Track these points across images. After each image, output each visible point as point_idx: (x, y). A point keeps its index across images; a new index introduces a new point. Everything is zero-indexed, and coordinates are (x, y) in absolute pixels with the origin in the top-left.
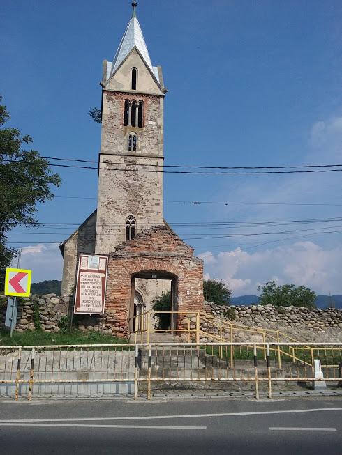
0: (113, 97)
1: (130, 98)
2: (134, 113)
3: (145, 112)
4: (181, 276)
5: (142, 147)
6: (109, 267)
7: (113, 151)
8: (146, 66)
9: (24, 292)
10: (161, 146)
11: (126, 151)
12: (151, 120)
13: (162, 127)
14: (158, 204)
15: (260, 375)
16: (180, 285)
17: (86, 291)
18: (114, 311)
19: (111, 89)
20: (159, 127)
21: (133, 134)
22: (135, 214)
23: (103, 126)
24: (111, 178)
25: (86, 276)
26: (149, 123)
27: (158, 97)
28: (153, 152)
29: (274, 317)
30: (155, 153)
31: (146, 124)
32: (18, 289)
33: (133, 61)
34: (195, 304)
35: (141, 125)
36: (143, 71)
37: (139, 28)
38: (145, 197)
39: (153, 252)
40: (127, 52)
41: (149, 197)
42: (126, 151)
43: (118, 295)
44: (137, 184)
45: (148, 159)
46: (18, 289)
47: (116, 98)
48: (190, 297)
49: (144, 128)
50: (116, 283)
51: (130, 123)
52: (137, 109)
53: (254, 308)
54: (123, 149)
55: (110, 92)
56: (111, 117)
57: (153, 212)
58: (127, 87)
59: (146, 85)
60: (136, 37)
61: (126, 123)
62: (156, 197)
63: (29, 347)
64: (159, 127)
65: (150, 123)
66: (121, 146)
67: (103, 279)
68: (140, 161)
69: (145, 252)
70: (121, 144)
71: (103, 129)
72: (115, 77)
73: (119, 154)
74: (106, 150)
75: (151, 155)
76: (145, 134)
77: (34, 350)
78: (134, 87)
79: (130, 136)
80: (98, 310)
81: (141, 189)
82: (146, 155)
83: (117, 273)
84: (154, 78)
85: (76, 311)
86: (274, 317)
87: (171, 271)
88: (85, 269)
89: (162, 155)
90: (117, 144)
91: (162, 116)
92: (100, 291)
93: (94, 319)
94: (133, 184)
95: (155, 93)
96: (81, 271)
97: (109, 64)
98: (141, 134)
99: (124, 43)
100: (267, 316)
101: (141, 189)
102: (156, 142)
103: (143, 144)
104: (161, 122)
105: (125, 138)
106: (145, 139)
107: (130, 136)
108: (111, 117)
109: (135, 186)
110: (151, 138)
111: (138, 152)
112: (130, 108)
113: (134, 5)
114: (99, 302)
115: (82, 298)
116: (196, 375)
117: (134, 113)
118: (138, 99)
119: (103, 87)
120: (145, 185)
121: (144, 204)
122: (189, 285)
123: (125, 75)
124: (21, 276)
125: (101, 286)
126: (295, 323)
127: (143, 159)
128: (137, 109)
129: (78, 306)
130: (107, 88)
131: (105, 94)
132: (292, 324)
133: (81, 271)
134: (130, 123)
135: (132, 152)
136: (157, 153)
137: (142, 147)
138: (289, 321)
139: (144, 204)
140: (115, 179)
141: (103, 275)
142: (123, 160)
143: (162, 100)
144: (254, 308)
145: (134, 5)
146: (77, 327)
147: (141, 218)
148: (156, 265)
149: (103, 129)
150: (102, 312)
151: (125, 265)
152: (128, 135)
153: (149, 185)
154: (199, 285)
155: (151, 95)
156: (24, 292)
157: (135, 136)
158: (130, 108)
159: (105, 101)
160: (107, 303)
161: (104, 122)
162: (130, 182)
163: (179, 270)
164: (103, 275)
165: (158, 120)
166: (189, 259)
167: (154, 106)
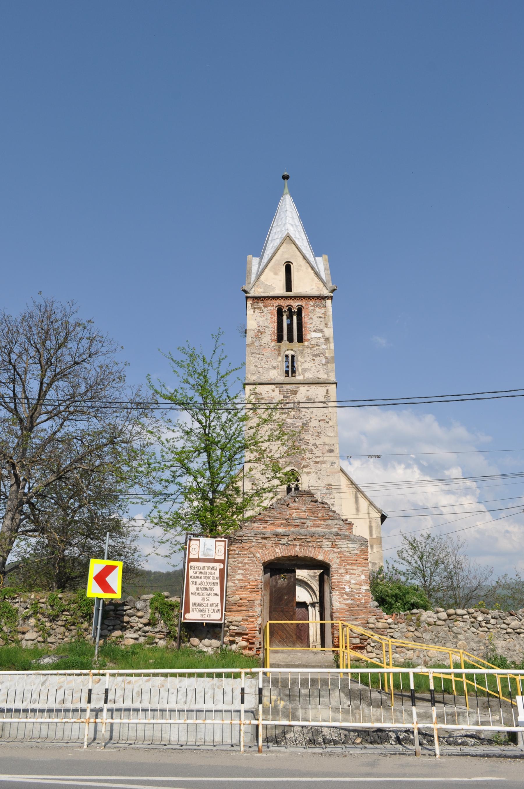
0: (261, 304)
1: (284, 303)
2: (290, 324)
3: (306, 321)
4: (334, 566)
5: (305, 371)
6: (228, 554)
7: (263, 379)
8: (305, 258)
9: (113, 592)
10: (332, 366)
11: (281, 378)
12: (315, 331)
13: (332, 340)
14: (331, 451)
15: (440, 718)
16: (335, 578)
17: (197, 588)
18: (240, 618)
19: (257, 294)
20: (327, 340)
21: (290, 353)
22: (298, 467)
23: (249, 346)
25: (197, 567)
26: (311, 335)
27: (323, 298)
28: (320, 376)
29: (483, 624)
30: (323, 376)
31: (308, 337)
32: (106, 588)
33: (287, 253)
34: (358, 606)
35: (300, 339)
36: (300, 266)
37: (293, 205)
38: (312, 441)
39: (292, 529)
40: (278, 241)
41: (318, 442)
42: (281, 378)
43: (245, 594)
44: (299, 423)
45: (313, 387)
46: (106, 588)
47: (265, 306)
48: (350, 595)
49: (306, 343)
50: (240, 577)
51: (285, 337)
52: (295, 318)
53: (451, 611)
54: (277, 375)
56: (259, 332)
57: (324, 462)
58: (280, 290)
59: (305, 284)
60: (288, 219)
61: (280, 339)
62: (327, 440)
63: (101, 672)
64: (327, 340)
65: (314, 335)
67: (222, 571)
68: (303, 392)
69: (280, 530)
70: (275, 368)
71: (247, 349)
72: (262, 278)
73: (272, 382)
74: (252, 378)
75: (317, 381)
77: (108, 675)
78: (289, 288)
79: (287, 356)
80: (215, 617)
81: (307, 431)
82: (310, 381)
83: (241, 562)
84: (317, 274)
85: (185, 619)
86: (483, 624)
87: (320, 557)
88: (196, 557)
89: (333, 379)
91: (331, 324)
92: (217, 589)
93: (212, 630)
95: (315, 293)
96: (190, 560)
97: (255, 261)
98: (302, 352)
99: (274, 230)
100: (472, 623)
101: (307, 431)
102: (324, 361)
103: (306, 366)
104: (329, 332)
105: (280, 358)
106: (308, 359)
108: (259, 332)
109: (298, 427)
111: (299, 378)
112: (285, 317)
113: (285, 177)
114: (217, 605)
115: (193, 599)
116: (340, 716)
117: (290, 324)
118: (295, 304)
119: (246, 292)
120: (312, 424)
121: (311, 451)
122: (347, 577)
123: (276, 274)
124: (109, 570)
125: (218, 581)
126: (519, 633)
127: (306, 387)
128: (295, 318)
129: (187, 611)
130: (252, 294)
132: (514, 637)
133: (190, 560)
134: (285, 337)
135: (290, 379)
136: (325, 376)
137: (305, 371)
138: (509, 630)
139: (311, 451)
141: (221, 566)
142: (277, 390)
143: (329, 302)
144: (451, 611)
145: (285, 177)
146: (188, 641)
147: (308, 473)
148: (298, 551)
149: (247, 349)
150: (221, 619)
151: (252, 550)
152: (283, 354)
153: (317, 424)
154: (363, 577)
155: (313, 297)
156: (113, 592)
157: (293, 357)
159: (250, 311)
160: (227, 607)
161: (249, 340)
162: (289, 421)
163: (331, 556)
164: (221, 566)
165: (326, 330)
166: (345, 537)
167: (319, 311)
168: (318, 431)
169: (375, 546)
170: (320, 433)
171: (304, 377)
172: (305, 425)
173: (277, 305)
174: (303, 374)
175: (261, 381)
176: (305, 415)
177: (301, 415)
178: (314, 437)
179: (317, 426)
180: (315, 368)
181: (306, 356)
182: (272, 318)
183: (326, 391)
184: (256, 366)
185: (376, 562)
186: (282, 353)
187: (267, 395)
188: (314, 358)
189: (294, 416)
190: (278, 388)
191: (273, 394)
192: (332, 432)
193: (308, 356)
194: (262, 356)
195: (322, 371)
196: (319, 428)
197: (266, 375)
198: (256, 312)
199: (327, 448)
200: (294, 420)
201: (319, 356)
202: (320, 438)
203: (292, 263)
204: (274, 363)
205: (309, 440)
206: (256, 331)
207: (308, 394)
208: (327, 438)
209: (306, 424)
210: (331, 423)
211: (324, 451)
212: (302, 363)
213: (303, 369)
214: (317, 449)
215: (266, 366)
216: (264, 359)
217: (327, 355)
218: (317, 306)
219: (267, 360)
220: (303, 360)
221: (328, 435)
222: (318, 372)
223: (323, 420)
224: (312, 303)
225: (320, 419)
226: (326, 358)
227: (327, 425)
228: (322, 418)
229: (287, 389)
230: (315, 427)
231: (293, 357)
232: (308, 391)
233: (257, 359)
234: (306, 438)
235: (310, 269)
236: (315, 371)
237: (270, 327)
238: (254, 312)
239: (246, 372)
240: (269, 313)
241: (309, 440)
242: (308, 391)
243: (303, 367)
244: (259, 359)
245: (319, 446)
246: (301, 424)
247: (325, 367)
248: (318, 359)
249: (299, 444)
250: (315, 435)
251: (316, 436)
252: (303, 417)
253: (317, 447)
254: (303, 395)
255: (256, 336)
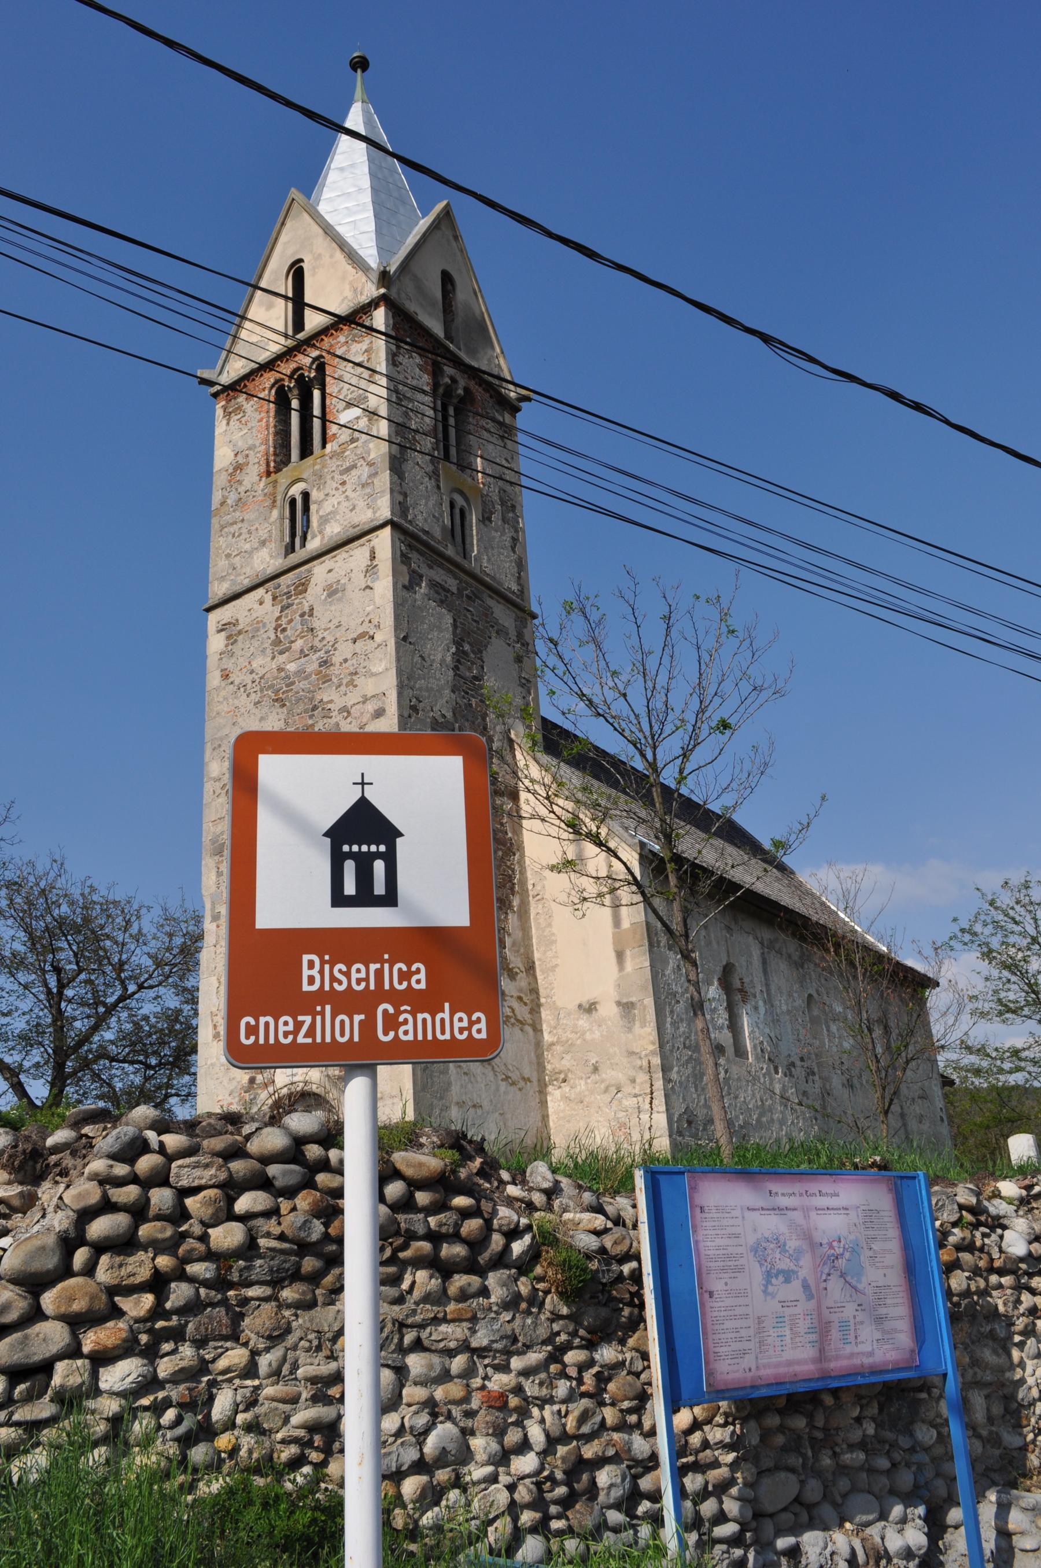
3: (331, 387)
5: (324, 520)
11: (277, 563)
21: (296, 490)
24: (236, 683)
30: (364, 517)
44: (312, 664)
45: (342, 554)
49: (329, 446)
55: (236, 387)
66: (264, 553)
70: (263, 543)
74: (219, 589)
75: (352, 532)
76: (333, 464)
79: (293, 502)
81: (326, 679)
82: (332, 544)
90: (250, 553)
94: (301, 673)
101: (326, 679)
103: (327, 507)
107: (293, 502)
109: (310, 675)
110: (348, 470)
111: (314, 544)
113: (361, 64)
118: (305, 360)
120: (337, 659)
127: (328, 562)
128: (317, 394)
131: (219, 412)
136: (369, 514)
140: (248, 679)
142: (268, 598)
158: (295, 404)
159: (220, 427)
162: (292, 667)
168: (352, 669)
169: (628, 953)
170: (356, 673)
171: (323, 538)
172: (325, 663)
173: (272, 381)
174: (320, 532)
175: (238, 588)
176: (323, 638)
177: (316, 643)
178: (343, 688)
179: (349, 656)
180: (346, 504)
181: (329, 482)
182: (260, 420)
183: (368, 554)
184: (228, 556)
185: (634, 999)
186: (279, 498)
187: (248, 620)
188: (345, 477)
189: (302, 651)
190: (270, 593)
191: (260, 611)
192: (381, 660)
193: (333, 478)
194: (239, 525)
195: (361, 504)
196: (354, 661)
197: (248, 571)
198: (231, 423)
199: (371, 707)
200: (303, 660)
201: (354, 466)
202: (356, 686)
203: (301, 260)
204: (263, 534)
205: (331, 701)
206: (230, 471)
207: (332, 578)
208: (371, 681)
209: (326, 662)
210: (378, 638)
211: (365, 720)
212: (320, 503)
213: (321, 517)
214: (349, 720)
215: (247, 546)
216: (244, 531)
217: (372, 456)
218: (354, 341)
219: (250, 532)
220: (321, 495)
221: (374, 670)
222: (351, 511)
223: (362, 635)
224: (342, 339)
225: (355, 635)
226: (370, 464)
227: (371, 645)
228: (360, 630)
229: (288, 586)
230: (346, 660)
231: (306, 496)
232: (330, 571)
233: (230, 537)
234: (325, 700)
235: (339, 256)
236: (347, 511)
237: (257, 443)
238: (228, 424)
239: (211, 578)
240: (256, 410)
241: (331, 701)
242: (330, 571)
243: (321, 513)
244: (233, 536)
245: (352, 711)
246: (315, 666)
247: (368, 490)
248: (352, 478)
249: (310, 722)
250: (344, 682)
251: (347, 685)
252: (319, 645)
253: (349, 713)
254: (319, 589)
255: (230, 481)
